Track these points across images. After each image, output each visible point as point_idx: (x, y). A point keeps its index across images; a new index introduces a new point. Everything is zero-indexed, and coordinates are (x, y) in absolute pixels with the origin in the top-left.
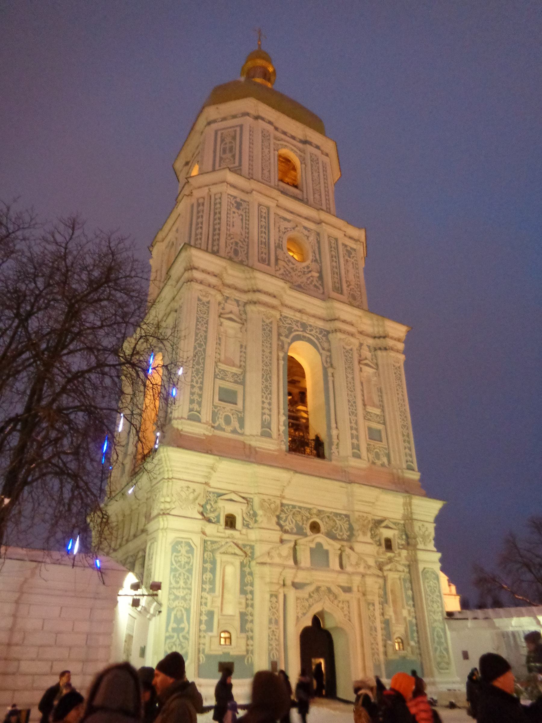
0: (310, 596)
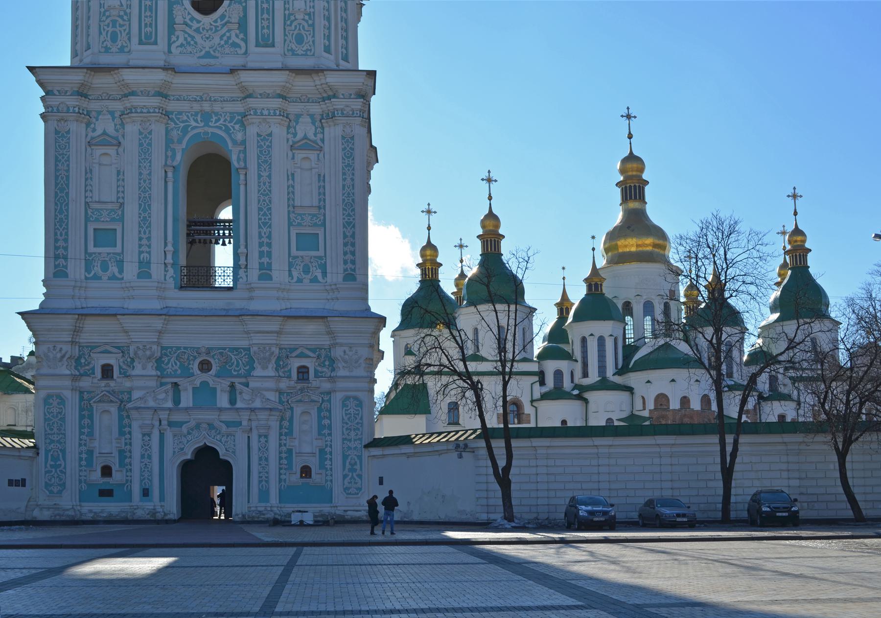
0: (189, 433)
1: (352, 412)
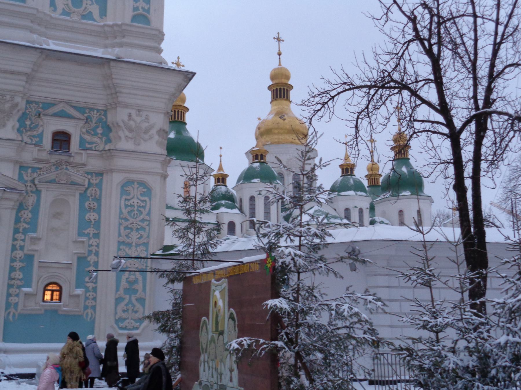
1: (135, 204)
